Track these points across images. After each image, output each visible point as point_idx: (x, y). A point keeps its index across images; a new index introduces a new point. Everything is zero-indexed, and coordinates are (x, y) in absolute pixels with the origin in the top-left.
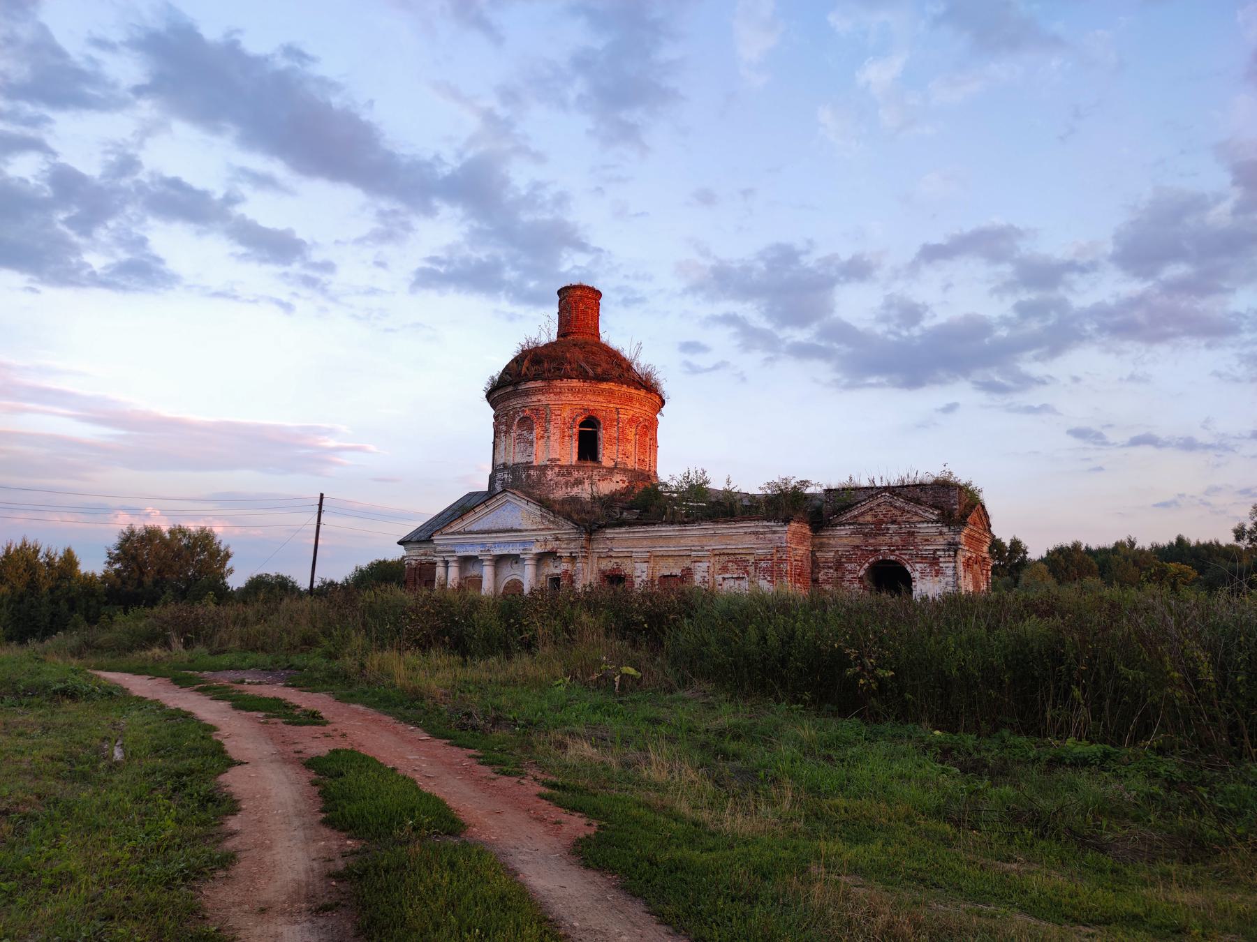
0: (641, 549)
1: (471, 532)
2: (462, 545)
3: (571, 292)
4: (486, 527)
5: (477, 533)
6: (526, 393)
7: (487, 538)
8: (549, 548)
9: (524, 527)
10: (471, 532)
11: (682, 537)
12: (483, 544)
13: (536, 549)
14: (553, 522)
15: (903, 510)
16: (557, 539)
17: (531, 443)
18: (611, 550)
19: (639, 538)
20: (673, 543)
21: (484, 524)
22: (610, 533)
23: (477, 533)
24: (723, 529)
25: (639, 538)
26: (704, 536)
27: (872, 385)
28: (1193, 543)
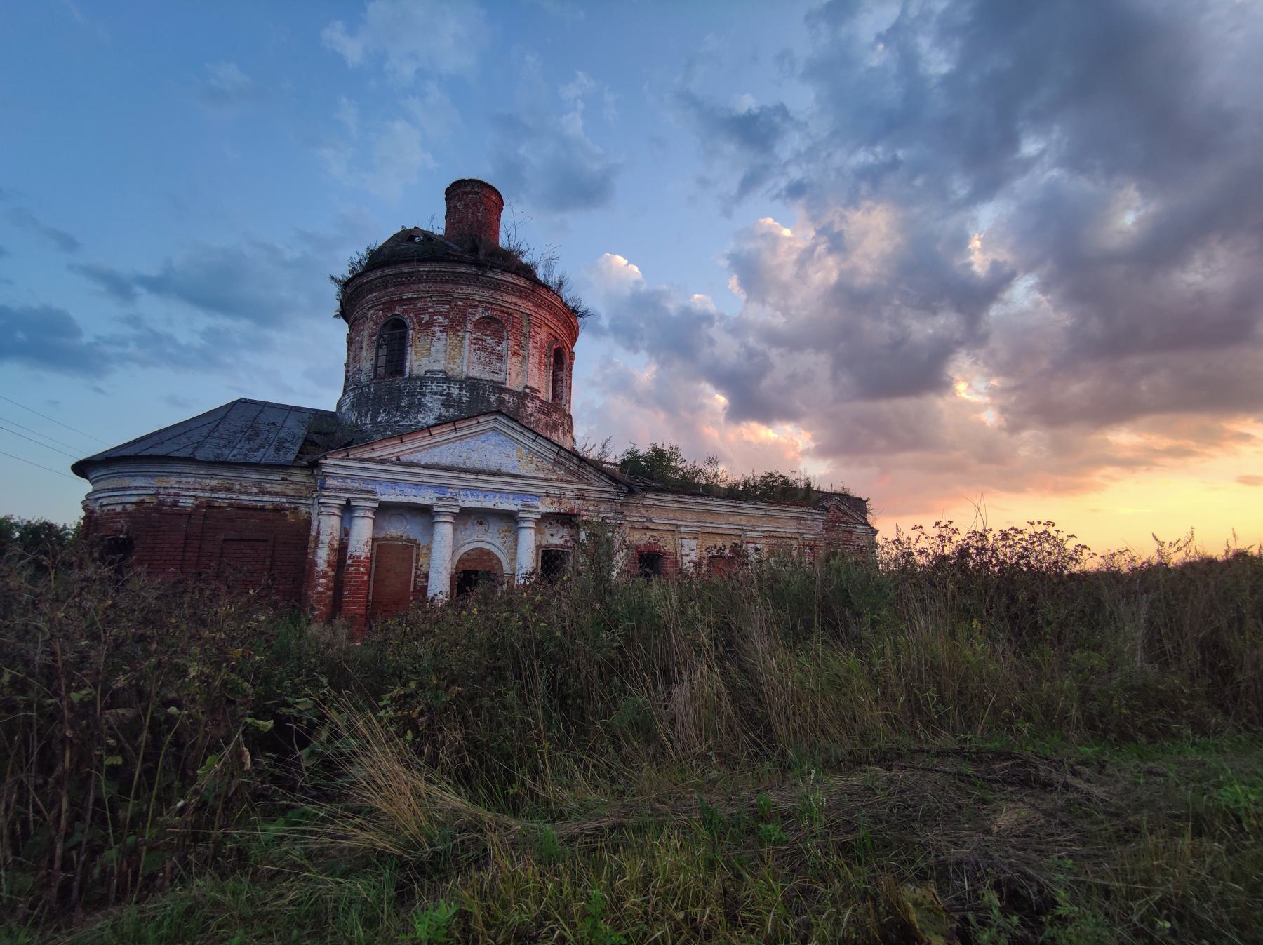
0: (689, 522)
1: (418, 465)
2: (393, 483)
3: (487, 192)
4: (447, 461)
5: (426, 466)
6: (497, 286)
7: (454, 480)
8: (565, 507)
9: (523, 472)
10: (418, 465)
11: (732, 514)
12: (441, 487)
13: (545, 507)
14: (573, 473)
15: (845, 513)
16: (581, 497)
17: (500, 357)
18: (650, 520)
19: (684, 510)
20: (721, 519)
21: (435, 456)
22: (650, 499)
23: (426, 466)
24: (775, 511)
25: (684, 510)
26: (753, 516)
27: (1130, 463)
28: (1091, 564)
